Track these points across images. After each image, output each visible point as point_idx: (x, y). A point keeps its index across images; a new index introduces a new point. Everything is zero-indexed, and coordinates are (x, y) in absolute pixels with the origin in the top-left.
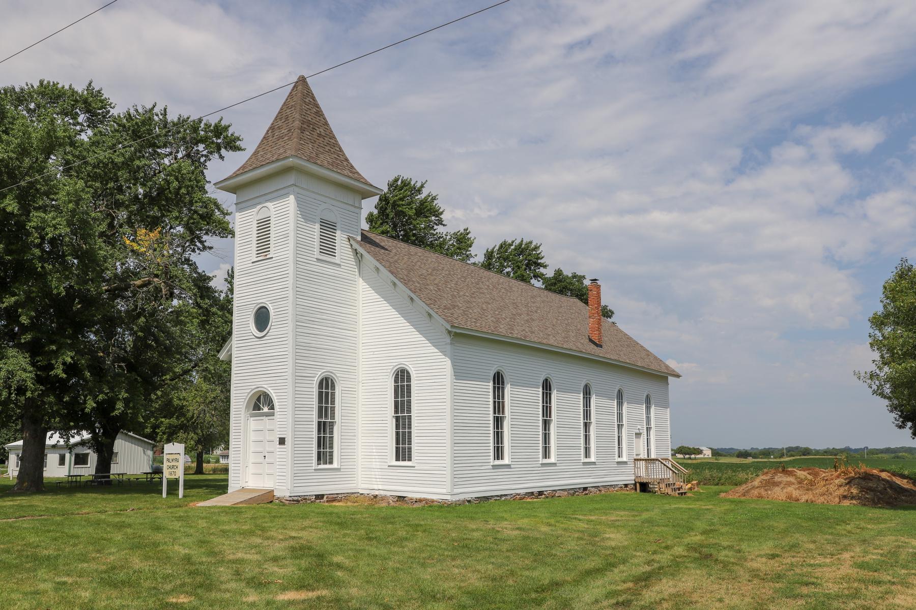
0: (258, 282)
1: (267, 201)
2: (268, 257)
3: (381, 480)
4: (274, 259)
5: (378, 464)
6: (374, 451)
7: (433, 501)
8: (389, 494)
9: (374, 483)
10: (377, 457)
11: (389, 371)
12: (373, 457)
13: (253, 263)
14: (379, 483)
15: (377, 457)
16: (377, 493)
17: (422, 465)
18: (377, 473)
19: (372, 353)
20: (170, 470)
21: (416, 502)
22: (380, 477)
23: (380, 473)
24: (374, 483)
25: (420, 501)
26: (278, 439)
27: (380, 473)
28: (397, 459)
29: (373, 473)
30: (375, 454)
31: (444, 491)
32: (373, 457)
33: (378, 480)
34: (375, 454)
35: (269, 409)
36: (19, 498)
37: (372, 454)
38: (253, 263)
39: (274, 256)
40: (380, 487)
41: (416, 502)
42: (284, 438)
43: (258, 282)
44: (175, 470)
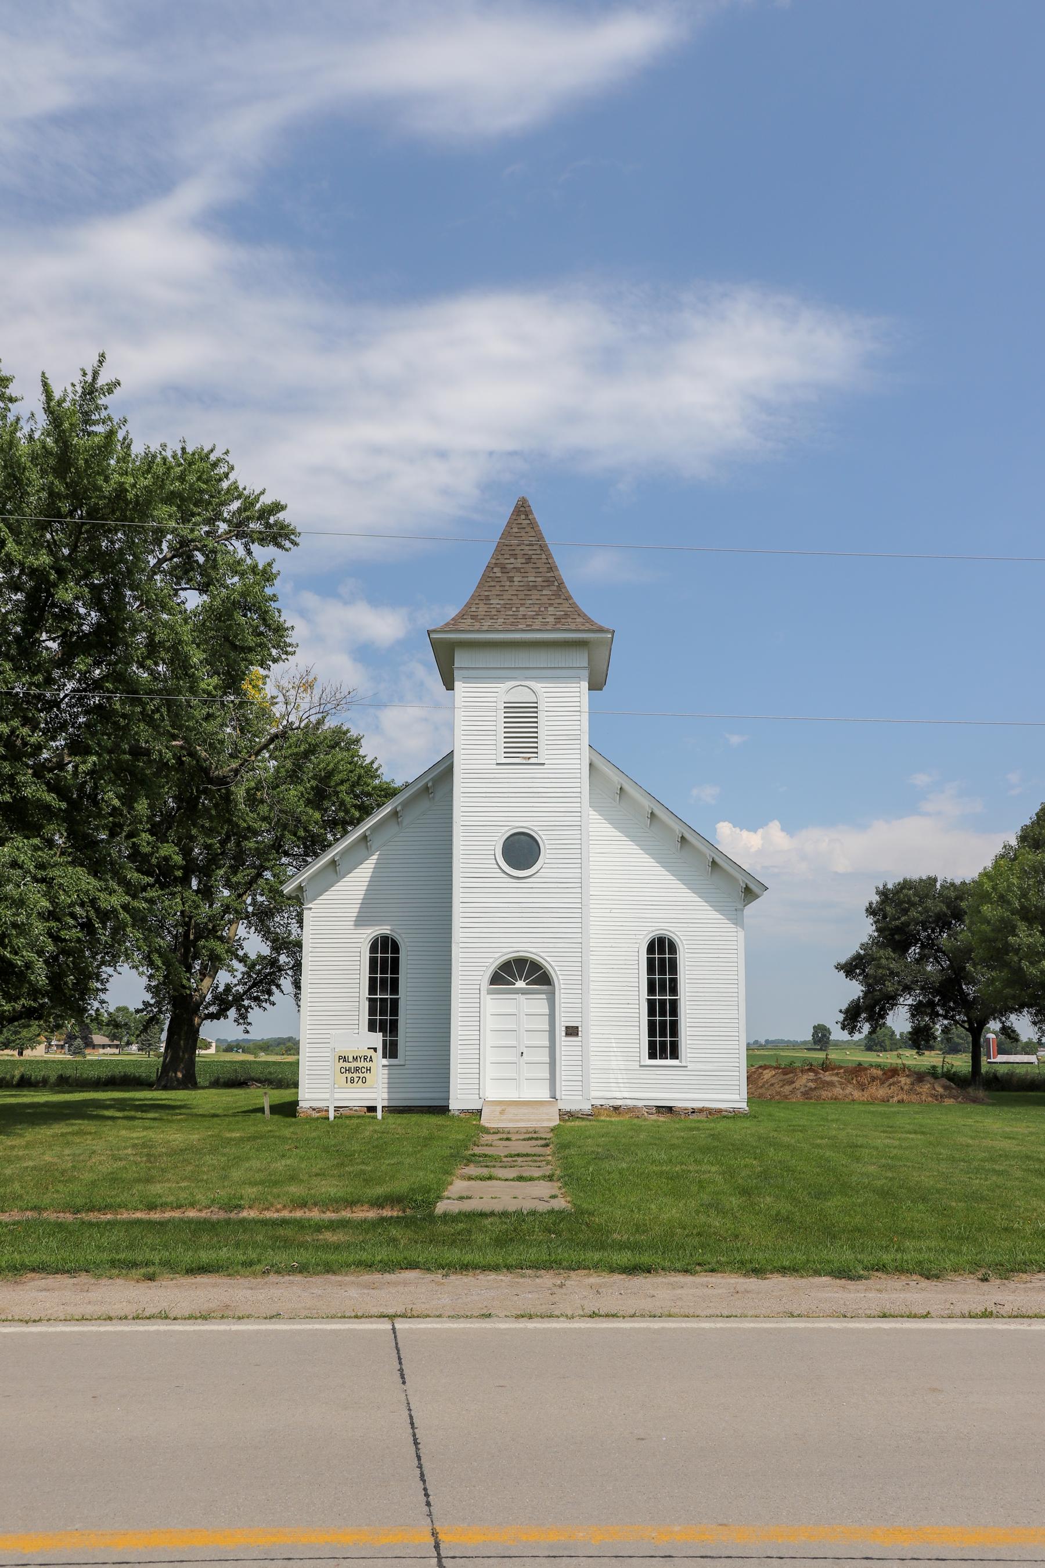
0: (510, 795)
1: (527, 678)
2: (532, 761)
3: (627, 1085)
4: (545, 766)
5: (622, 1063)
6: (614, 1045)
7: (720, 1111)
8: (640, 1104)
9: (614, 1089)
10: (619, 1054)
11: (641, 937)
12: (612, 1054)
13: (498, 764)
14: (622, 1089)
15: (619, 1054)
16: (619, 1103)
17: (698, 1064)
18: (620, 1076)
19: (609, 911)
20: (349, 1075)
21: (693, 1112)
22: (626, 1081)
23: (625, 1076)
24: (614, 1089)
25: (701, 1110)
26: (564, 1029)
27: (625, 1076)
28: (652, 1055)
29: (612, 1076)
30: (615, 1049)
31: (737, 1097)
32: (612, 1054)
33: (622, 1085)
34: (615, 1049)
35: (527, 984)
36: (77, 1122)
37: (611, 1049)
38: (498, 764)
39: (546, 762)
40: (626, 1095)
41: (693, 1112)
42: (577, 1027)
43: (510, 795)
44: (365, 1075)
